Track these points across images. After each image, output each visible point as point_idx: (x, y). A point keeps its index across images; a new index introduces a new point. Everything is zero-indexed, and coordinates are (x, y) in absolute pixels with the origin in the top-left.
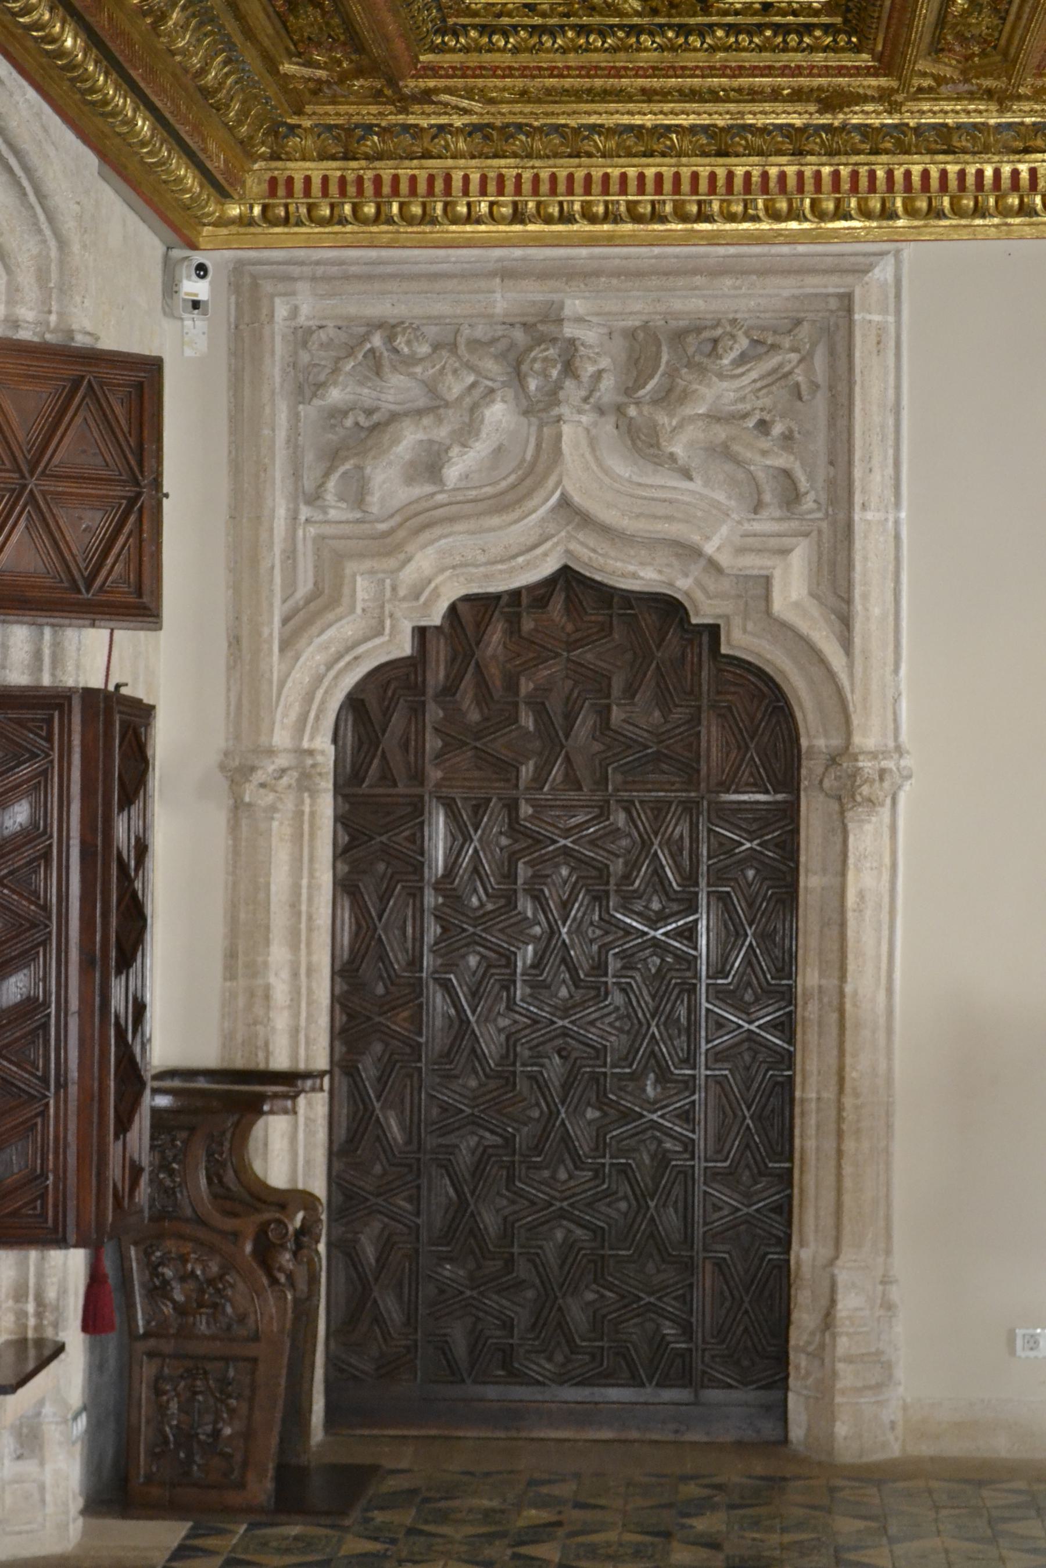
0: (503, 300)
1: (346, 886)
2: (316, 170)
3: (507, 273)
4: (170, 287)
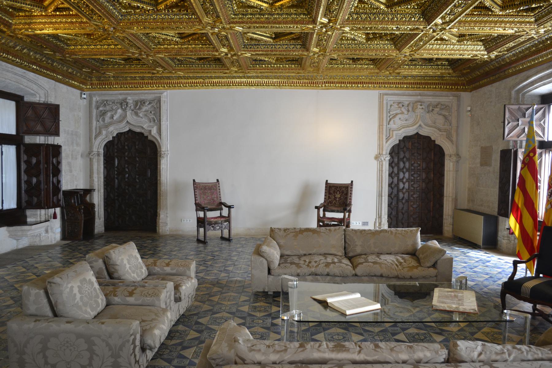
0: (121, 97)
1: (105, 167)
2: (96, 82)
3: (120, 94)
4: (81, 96)
